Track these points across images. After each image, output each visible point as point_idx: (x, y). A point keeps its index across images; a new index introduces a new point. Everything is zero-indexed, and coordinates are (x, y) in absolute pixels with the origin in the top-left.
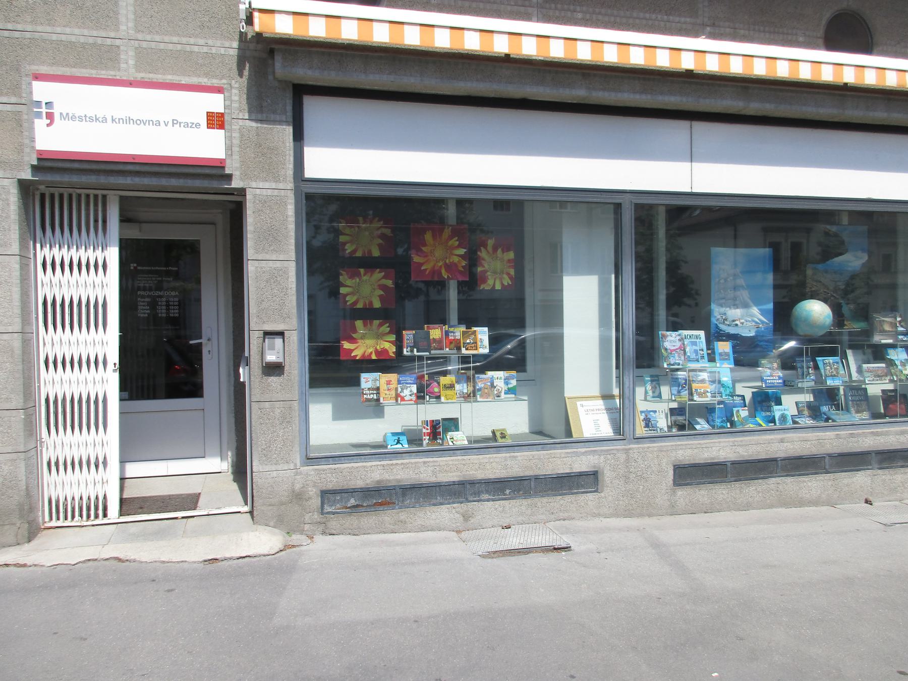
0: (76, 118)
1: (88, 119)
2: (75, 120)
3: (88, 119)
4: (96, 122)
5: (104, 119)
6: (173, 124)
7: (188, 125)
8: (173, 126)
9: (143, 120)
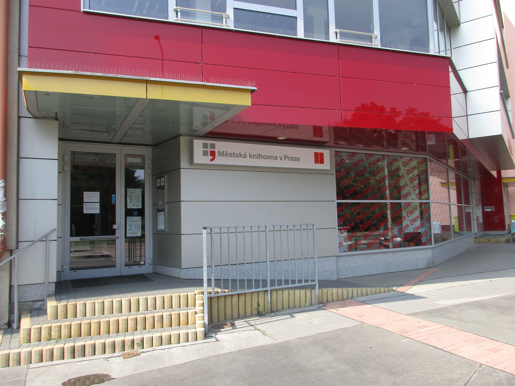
0: (228, 155)
1: (235, 156)
2: (228, 156)
3: (235, 156)
4: (240, 157)
5: (245, 155)
6: (285, 158)
7: (293, 159)
8: (285, 160)
9: (267, 156)
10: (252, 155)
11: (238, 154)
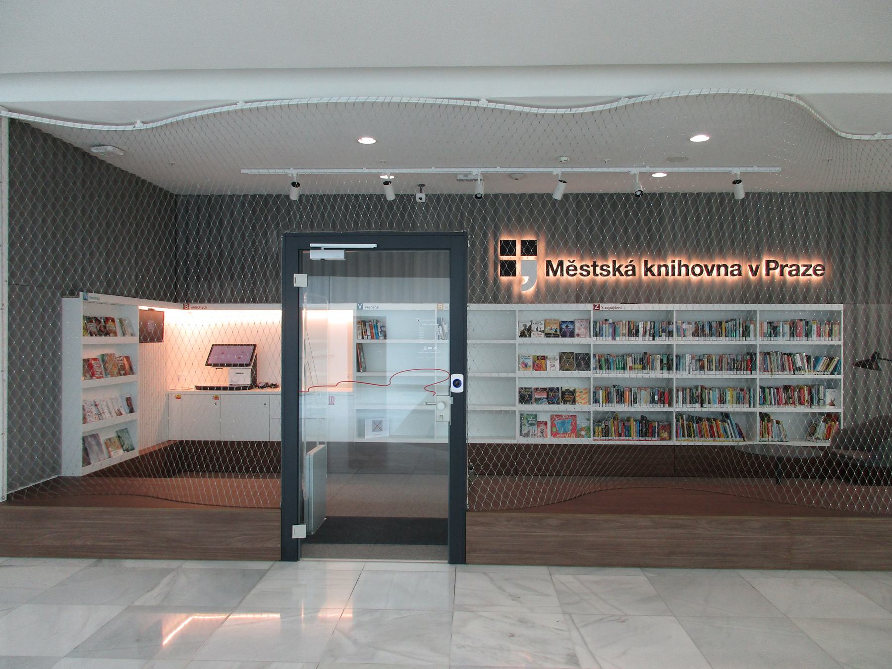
0: (576, 269)
2: (575, 274)
3: (598, 271)
4: (614, 275)
10: (652, 266)
11: (609, 267)
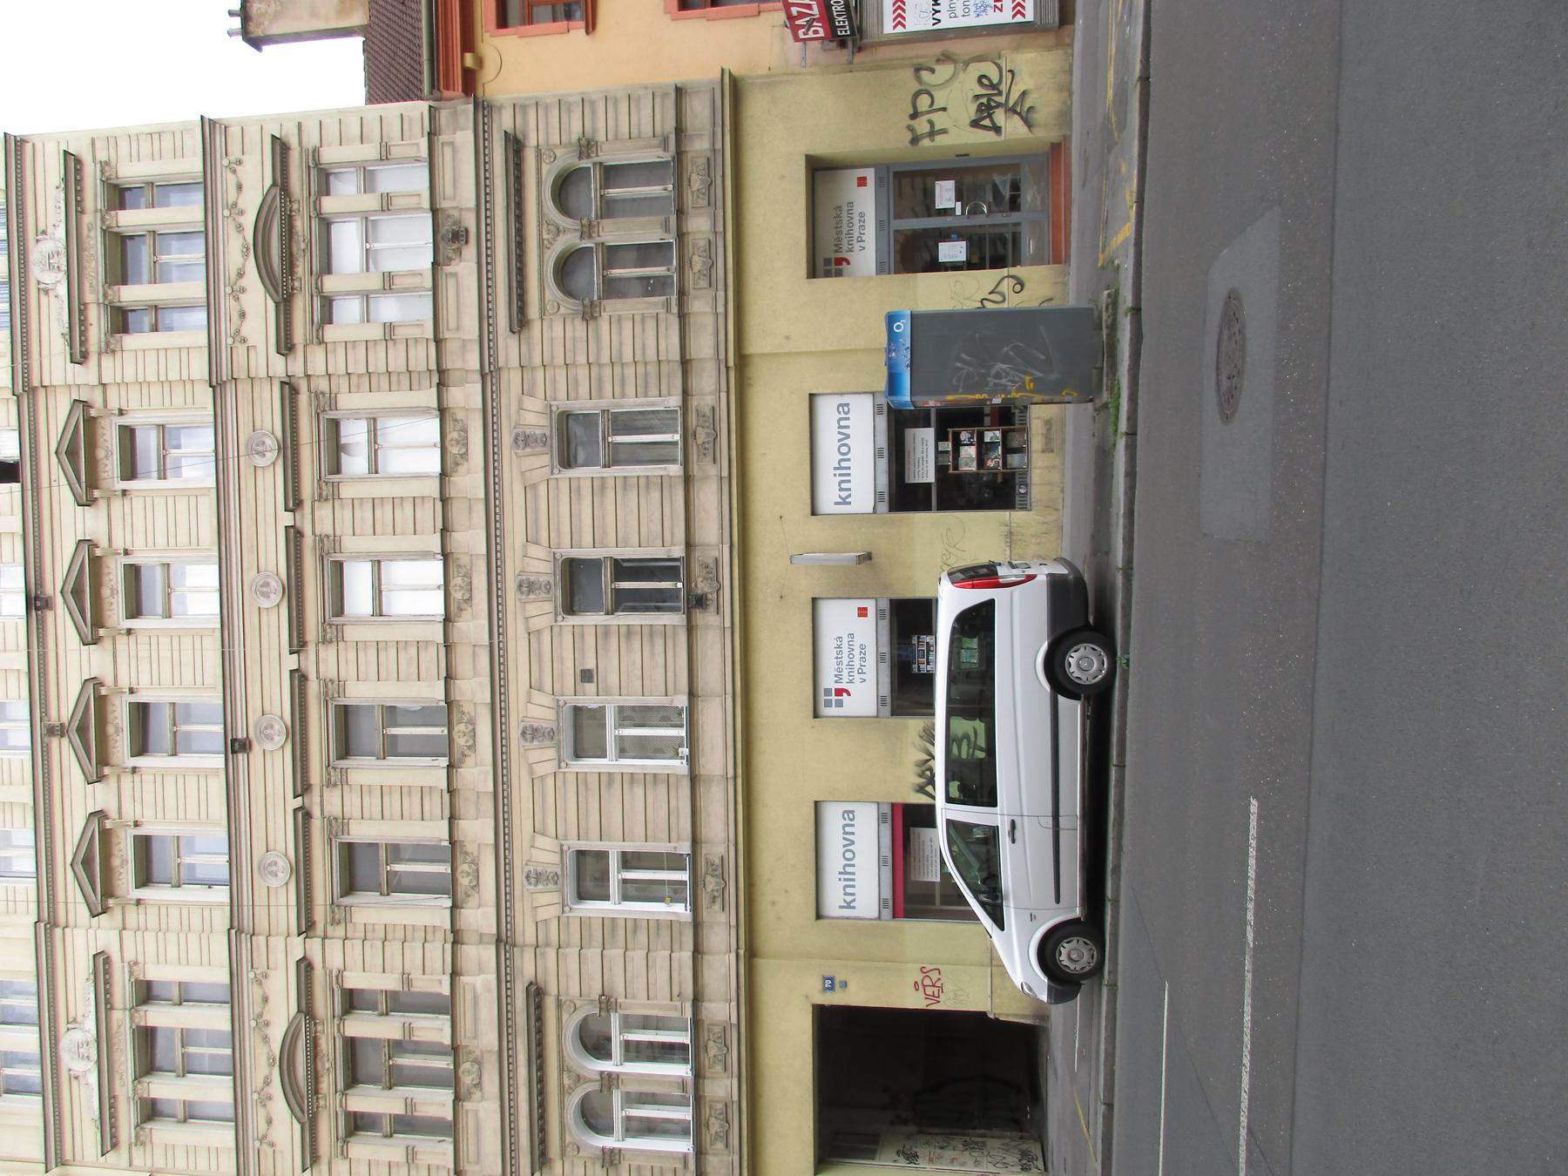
9: (839, 441)
